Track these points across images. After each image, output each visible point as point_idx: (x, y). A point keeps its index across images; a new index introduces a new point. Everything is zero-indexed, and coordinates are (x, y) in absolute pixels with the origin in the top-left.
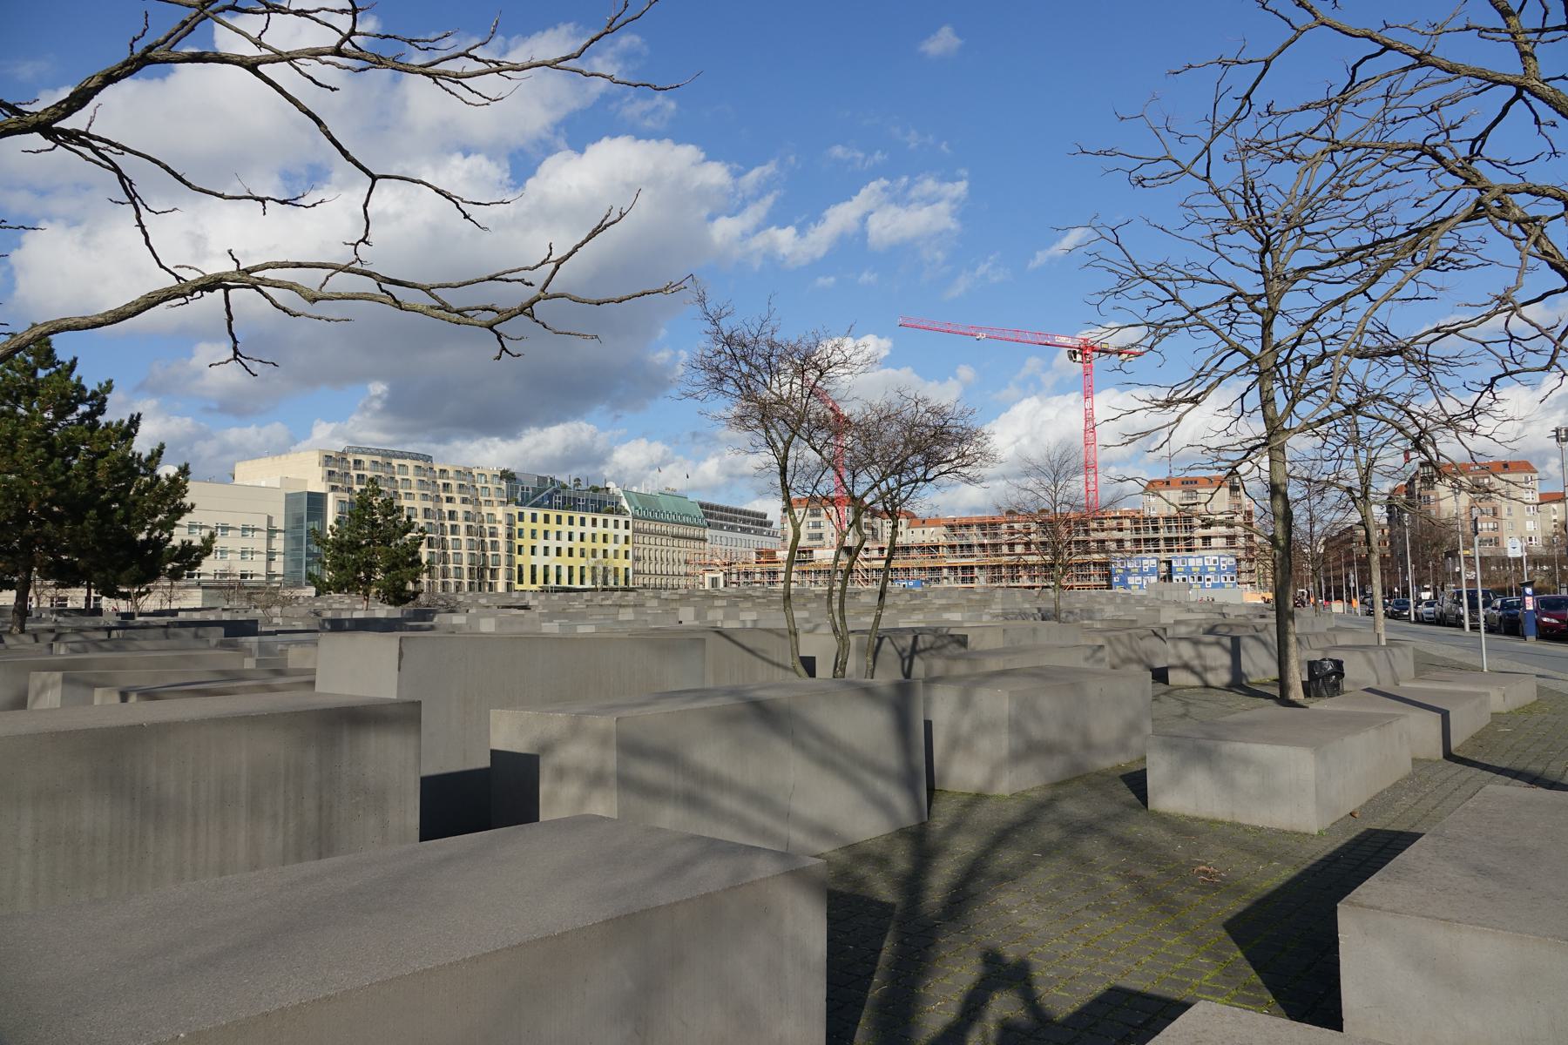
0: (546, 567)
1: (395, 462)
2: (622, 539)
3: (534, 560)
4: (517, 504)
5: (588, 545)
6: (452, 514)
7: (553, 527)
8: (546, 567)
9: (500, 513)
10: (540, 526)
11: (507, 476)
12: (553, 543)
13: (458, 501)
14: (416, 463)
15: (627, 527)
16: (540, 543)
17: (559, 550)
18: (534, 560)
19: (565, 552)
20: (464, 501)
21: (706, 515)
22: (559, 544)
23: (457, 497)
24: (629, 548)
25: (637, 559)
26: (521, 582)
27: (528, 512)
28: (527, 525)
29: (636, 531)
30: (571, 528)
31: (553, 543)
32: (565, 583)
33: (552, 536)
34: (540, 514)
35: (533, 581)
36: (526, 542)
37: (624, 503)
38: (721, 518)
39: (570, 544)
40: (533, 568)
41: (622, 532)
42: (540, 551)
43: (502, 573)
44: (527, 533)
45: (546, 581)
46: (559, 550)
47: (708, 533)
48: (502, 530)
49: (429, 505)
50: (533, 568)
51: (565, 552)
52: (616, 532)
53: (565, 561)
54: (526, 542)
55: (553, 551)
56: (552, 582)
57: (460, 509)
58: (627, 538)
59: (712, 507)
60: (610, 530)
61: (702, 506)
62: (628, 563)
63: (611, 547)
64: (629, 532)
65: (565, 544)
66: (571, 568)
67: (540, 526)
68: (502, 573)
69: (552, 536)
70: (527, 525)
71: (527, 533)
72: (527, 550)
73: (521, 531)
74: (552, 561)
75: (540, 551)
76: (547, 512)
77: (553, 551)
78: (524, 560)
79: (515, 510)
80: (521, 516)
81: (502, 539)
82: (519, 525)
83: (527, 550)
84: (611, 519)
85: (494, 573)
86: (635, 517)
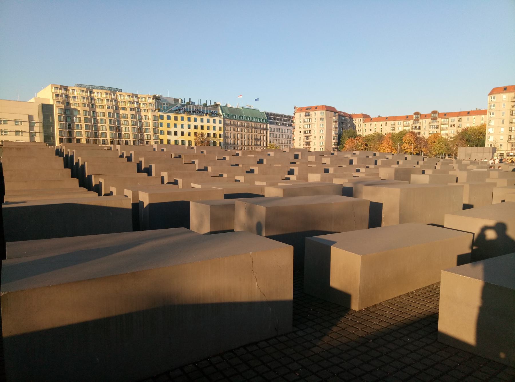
2: (217, 128)
4: (159, 111)
5: (199, 131)
10: (172, 122)
11: (156, 98)
13: (128, 109)
14: (105, 91)
15: (220, 122)
21: (269, 118)
22: (183, 130)
25: (226, 137)
27: (165, 115)
28: (165, 121)
29: (224, 124)
30: (189, 123)
33: (179, 126)
36: (165, 129)
37: (220, 112)
38: (278, 120)
39: (189, 130)
41: (217, 125)
46: (183, 134)
47: (269, 126)
49: (111, 111)
51: (186, 134)
52: (214, 125)
53: (186, 138)
54: (165, 129)
58: (220, 128)
59: (271, 114)
60: (211, 124)
61: (267, 114)
63: (212, 132)
64: (222, 125)
65: (186, 130)
67: (172, 122)
69: (179, 126)
70: (165, 121)
71: (165, 125)
77: (179, 134)
79: (158, 114)
84: (211, 119)
86: (224, 118)
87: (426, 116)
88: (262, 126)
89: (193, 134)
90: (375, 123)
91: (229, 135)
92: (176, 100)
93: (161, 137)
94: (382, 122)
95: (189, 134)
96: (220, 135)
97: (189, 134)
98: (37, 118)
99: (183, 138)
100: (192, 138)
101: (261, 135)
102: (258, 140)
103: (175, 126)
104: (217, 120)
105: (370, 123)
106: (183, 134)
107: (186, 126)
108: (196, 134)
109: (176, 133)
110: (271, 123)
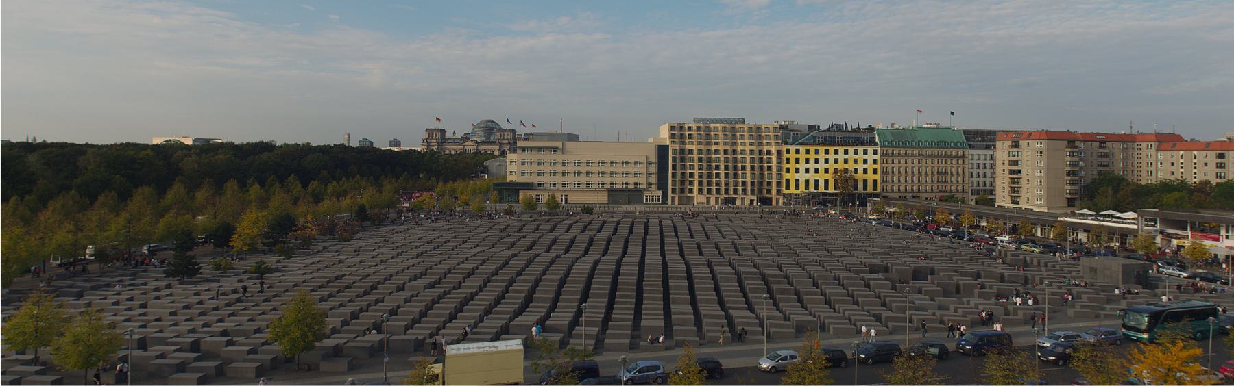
1: (712, 126)
3: (797, 176)
4: (786, 144)
5: (841, 166)
9: (773, 149)
15: (875, 152)
16: (802, 166)
18: (797, 176)
21: (968, 139)
24: (877, 167)
25: (884, 173)
26: (788, 187)
27: (793, 148)
29: (882, 155)
32: (822, 189)
33: (812, 161)
34: (802, 149)
36: (792, 165)
40: (797, 180)
43: (774, 184)
46: (817, 171)
48: (774, 158)
49: (728, 147)
50: (797, 180)
54: (792, 165)
56: (812, 189)
58: (875, 162)
61: (965, 132)
62: (877, 177)
64: (877, 157)
68: (774, 184)
69: (812, 161)
72: (793, 170)
78: (792, 176)
79: (784, 148)
80: (788, 151)
81: (774, 164)
83: (793, 170)
85: (769, 184)
88: (954, 153)
91: (889, 170)
92: (811, 128)
93: (786, 176)
95: (826, 171)
96: (875, 171)
97: (826, 171)
98: (654, 159)
99: (817, 176)
100: (830, 176)
101: (951, 166)
102: (946, 173)
103: (807, 161)
104: (870, 149)
106: (817, 171)
107: (822, 161)
109: (807, 171)
110: (971, 147)
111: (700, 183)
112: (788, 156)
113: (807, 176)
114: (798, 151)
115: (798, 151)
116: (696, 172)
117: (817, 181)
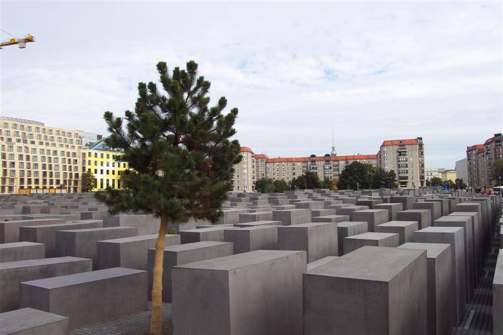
0: (102, 180)
6: (55, 152)
7: (105, 160)
8: (102, 180)
12: (105, 168)
17: (108, 172)
19: (111, 172)
20: (62, 145)
23: (58, 144)
27: (93, 152)
28: (93, 159)
31: (105, 168)
35: (96, 187)
42: (99, 172)
44: (93, 163)
45: (102, 187)
46: (108, 172)
51: (111, 172)
55: (105, 172)
57: (59, 150)
66: (113, 180)
67: (99, 159)
69: (105, 164)
71: (93, 163)
73: (89, 162)
74: (105, 177)
75: (99, 172)
76: (102, 152)
77: (105, 172)
79: (87, 151)
80: (90, 154)
82: (87, 159)
87: (320, 159)
89: (116, 173)
90: (277, 163)
94: (283, 163)
95: (113, 172)
97: (113, 172)
105: (272, 164)
108: (119, 171)
111: (22, 181)
112: (89, 159)
113: (102, 176)
114: (96, 155)
115: (96, 155)
116: (17, 168)
117: (108, 180)
